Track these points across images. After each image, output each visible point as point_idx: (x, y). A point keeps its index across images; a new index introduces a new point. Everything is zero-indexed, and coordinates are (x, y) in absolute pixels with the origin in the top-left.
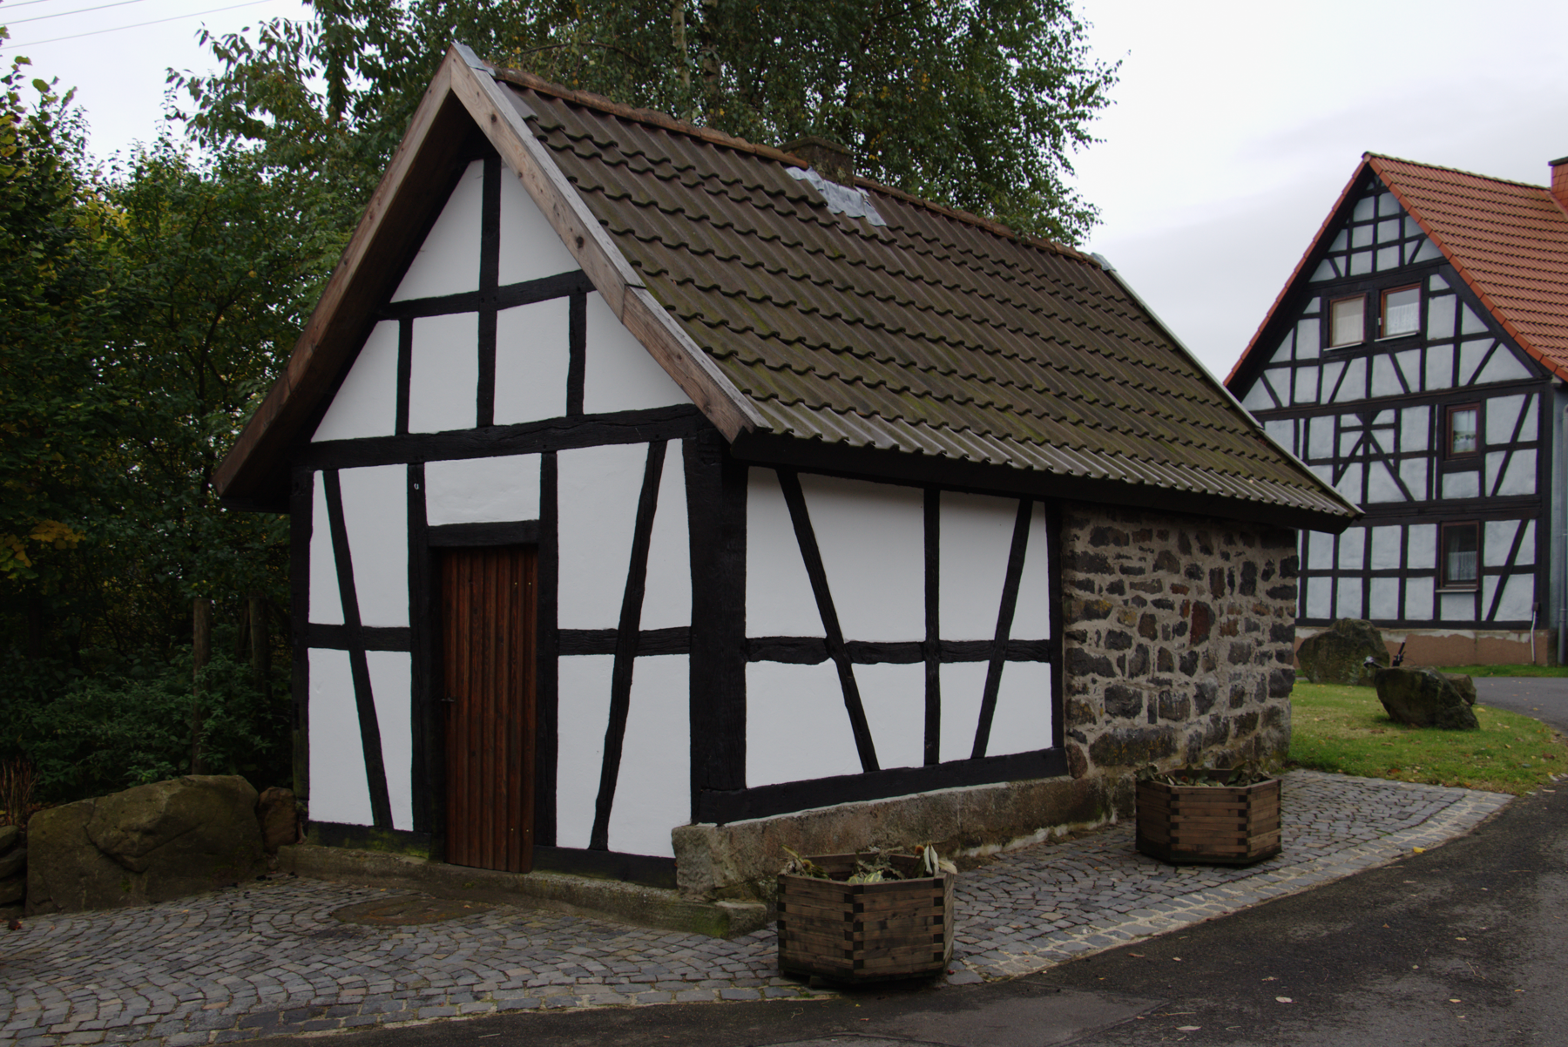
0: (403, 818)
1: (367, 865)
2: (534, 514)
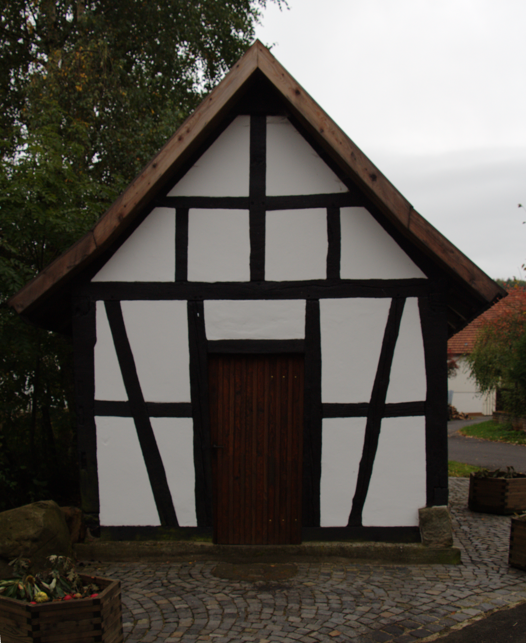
0: (187, 516)
1: (164, 549)
2: (300, 334)
